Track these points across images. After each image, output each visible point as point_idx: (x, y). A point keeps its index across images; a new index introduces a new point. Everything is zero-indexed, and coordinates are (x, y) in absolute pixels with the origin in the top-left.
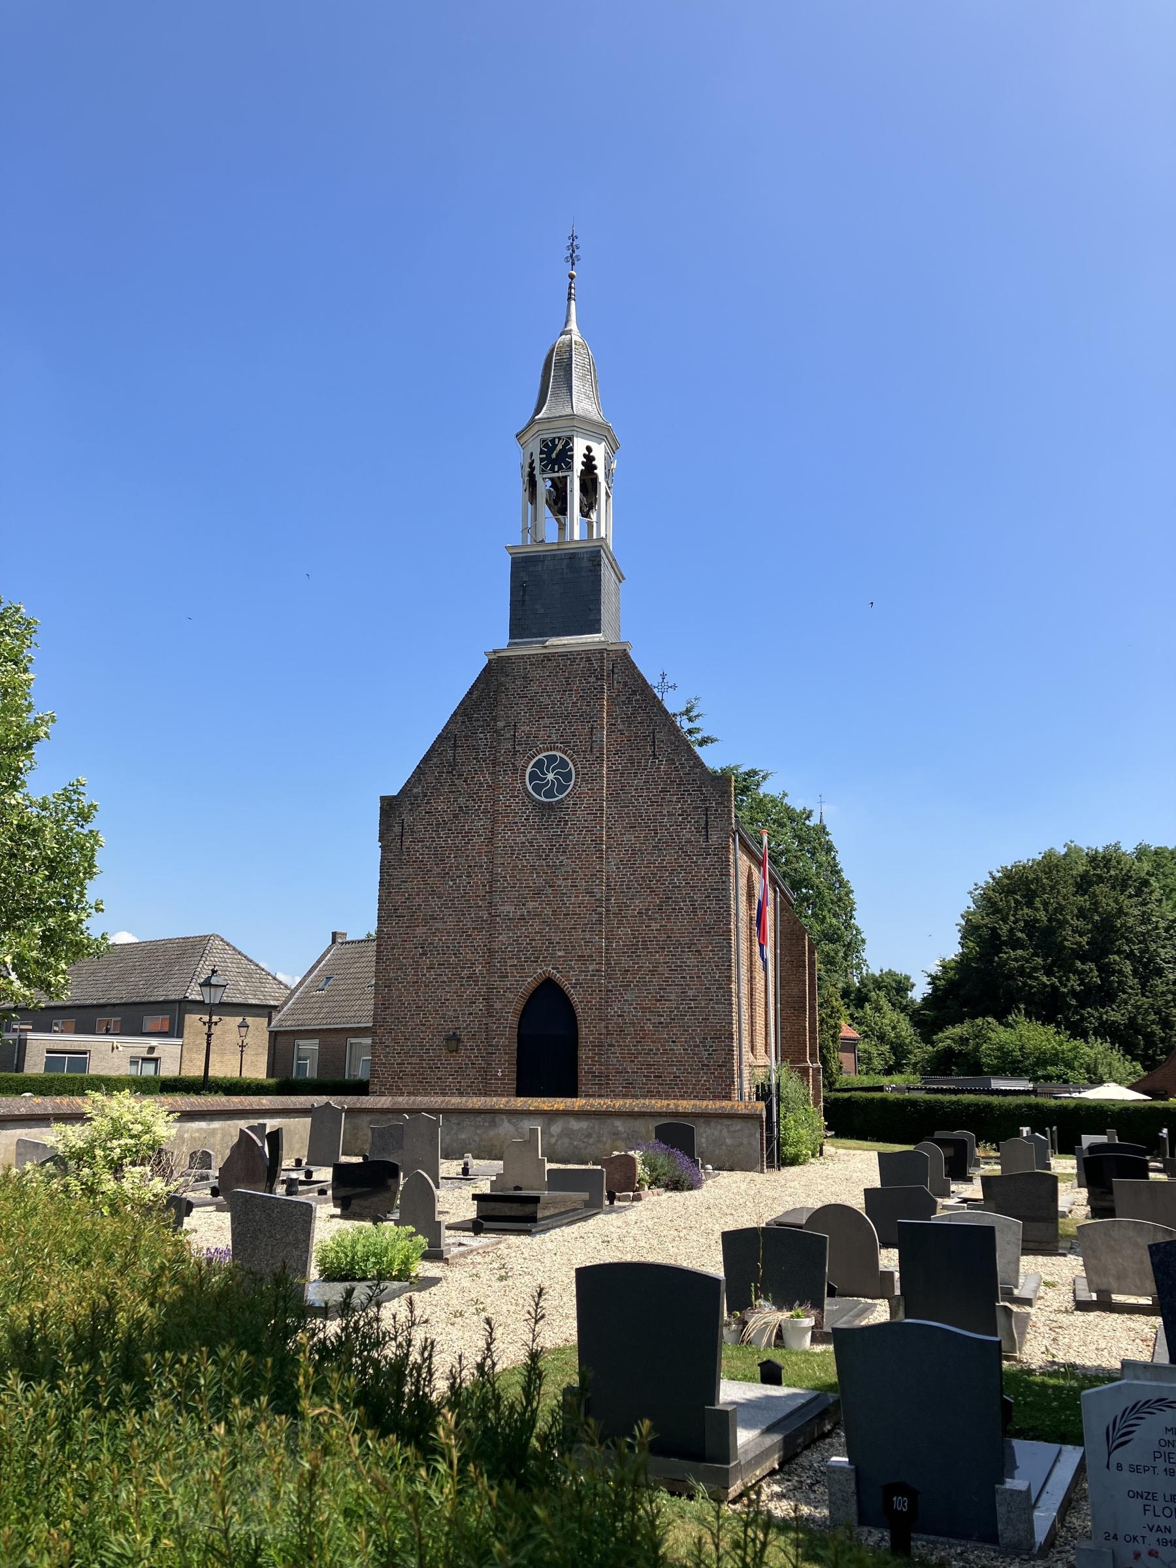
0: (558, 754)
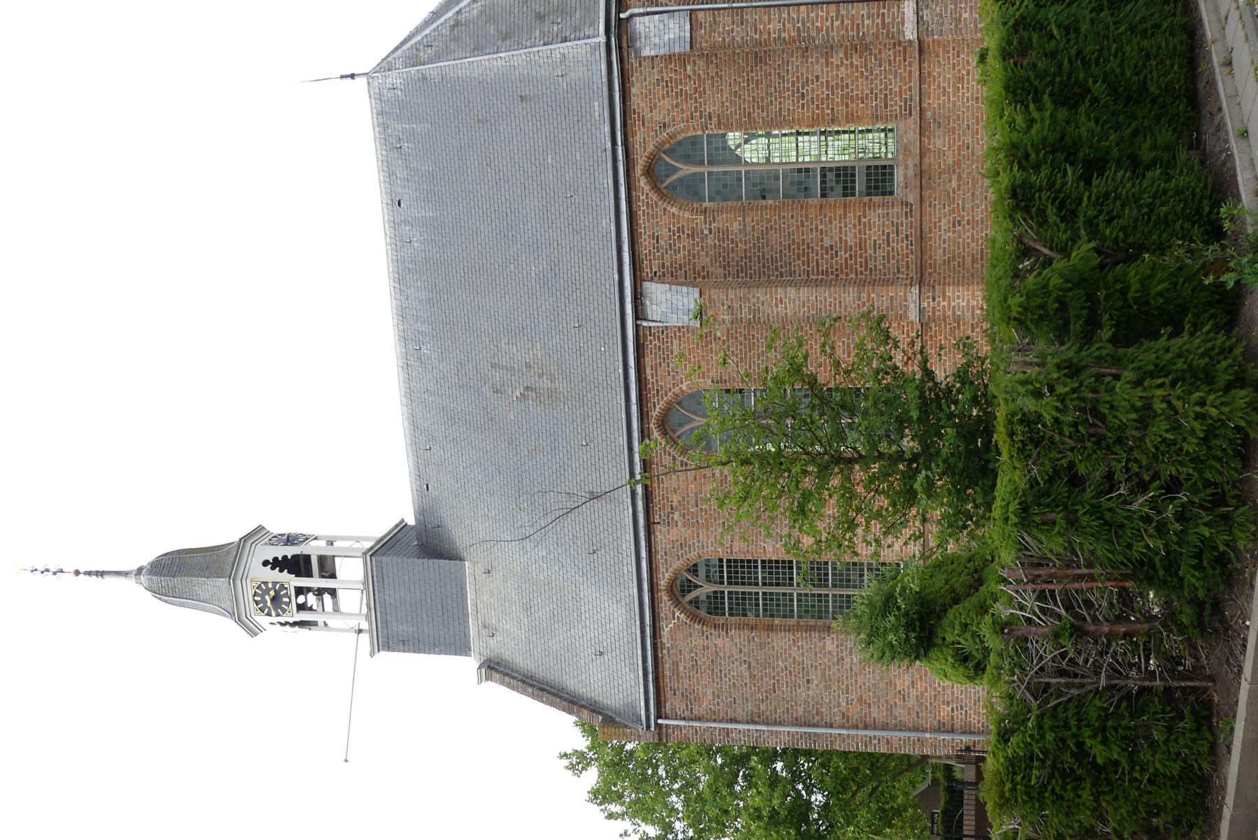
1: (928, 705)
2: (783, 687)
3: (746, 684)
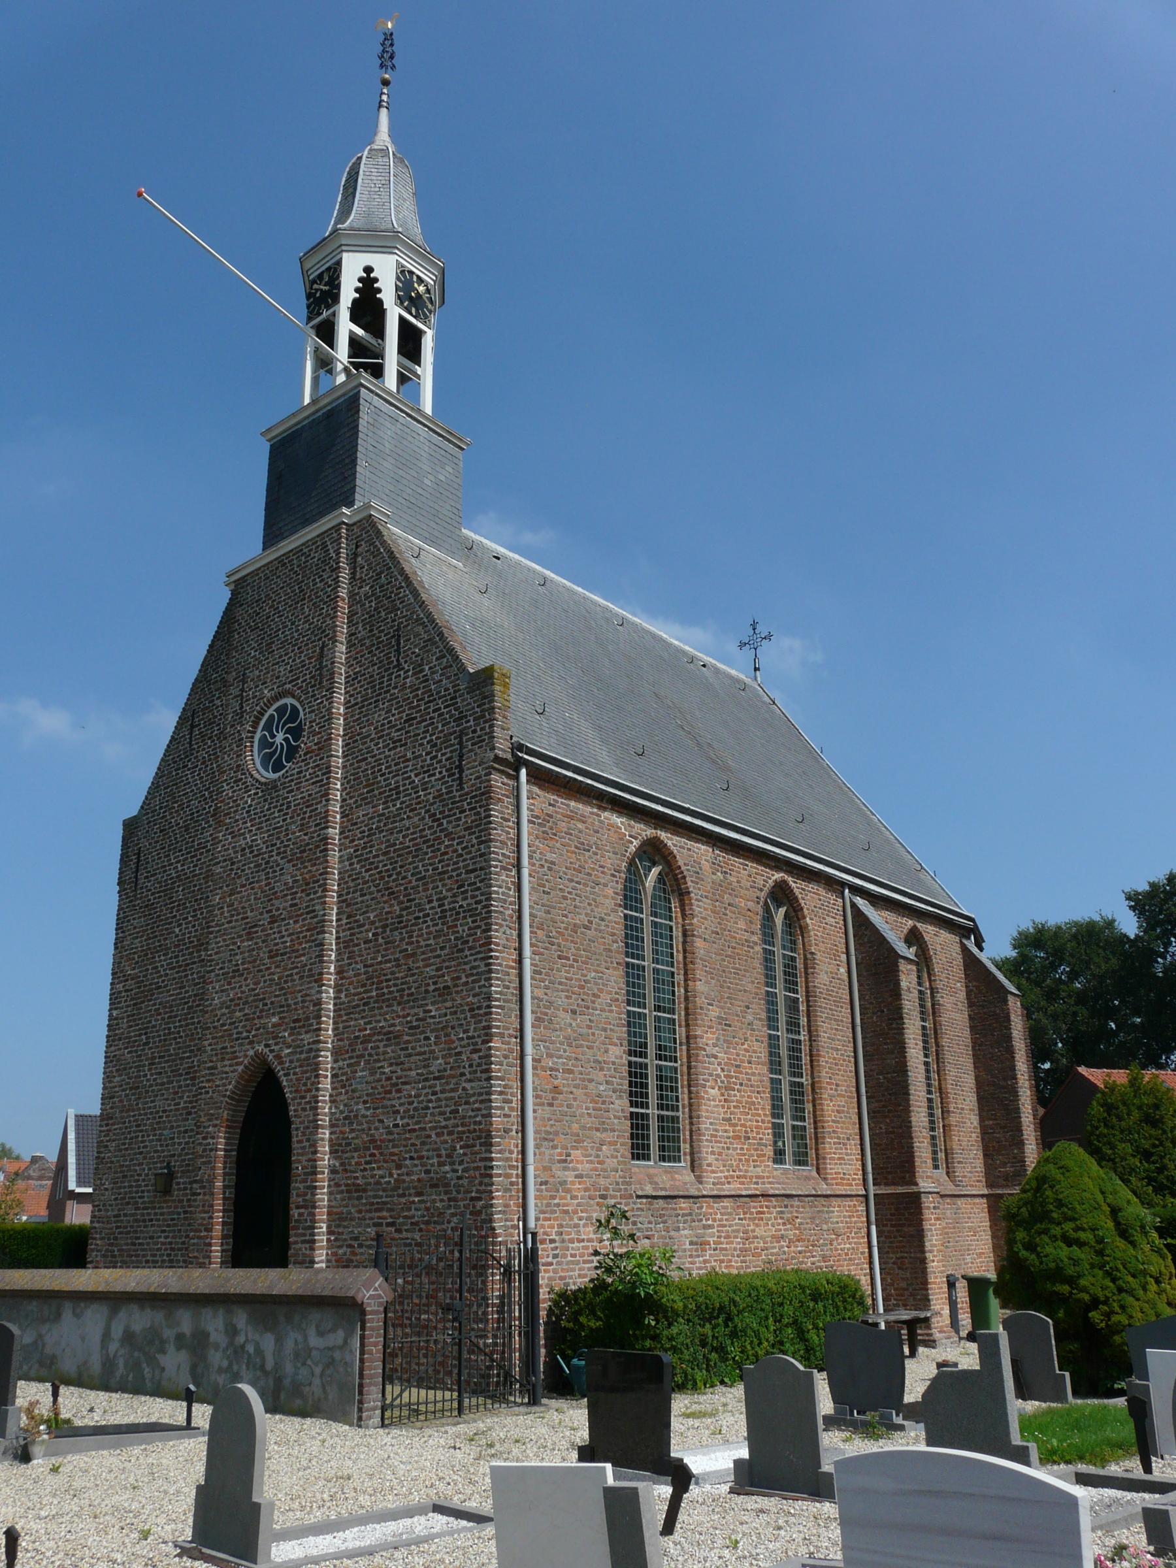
0: (289, 701)
1: (556, 1201)
2: (566, 972)
3: (566, 916)
